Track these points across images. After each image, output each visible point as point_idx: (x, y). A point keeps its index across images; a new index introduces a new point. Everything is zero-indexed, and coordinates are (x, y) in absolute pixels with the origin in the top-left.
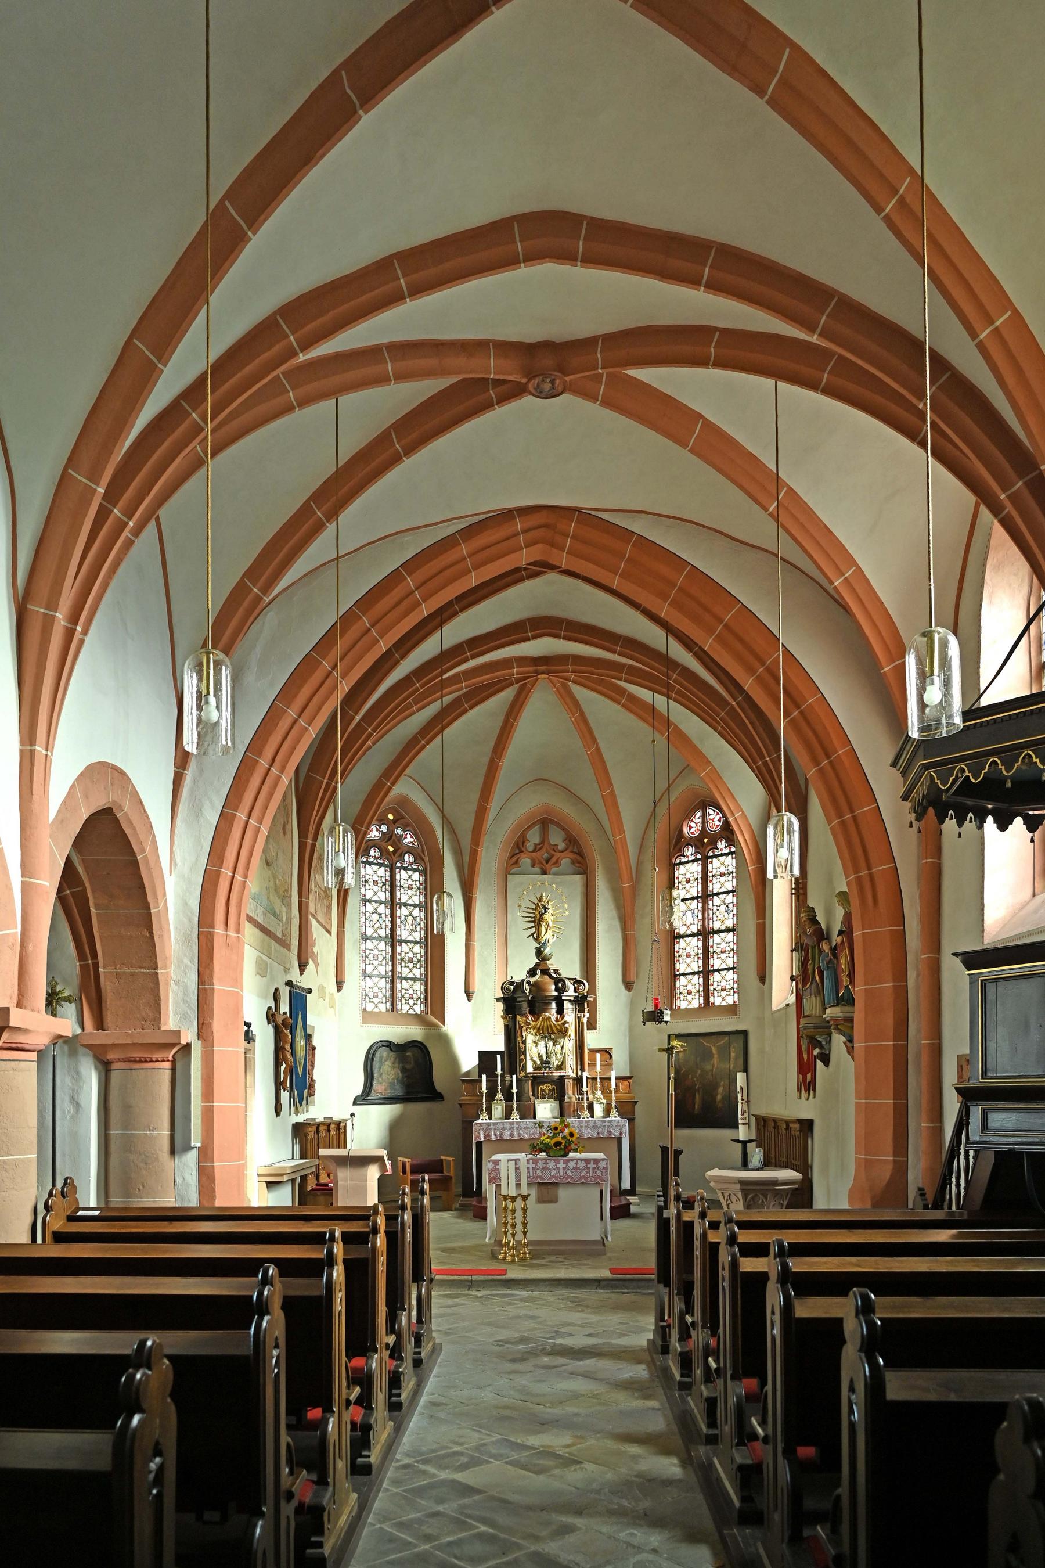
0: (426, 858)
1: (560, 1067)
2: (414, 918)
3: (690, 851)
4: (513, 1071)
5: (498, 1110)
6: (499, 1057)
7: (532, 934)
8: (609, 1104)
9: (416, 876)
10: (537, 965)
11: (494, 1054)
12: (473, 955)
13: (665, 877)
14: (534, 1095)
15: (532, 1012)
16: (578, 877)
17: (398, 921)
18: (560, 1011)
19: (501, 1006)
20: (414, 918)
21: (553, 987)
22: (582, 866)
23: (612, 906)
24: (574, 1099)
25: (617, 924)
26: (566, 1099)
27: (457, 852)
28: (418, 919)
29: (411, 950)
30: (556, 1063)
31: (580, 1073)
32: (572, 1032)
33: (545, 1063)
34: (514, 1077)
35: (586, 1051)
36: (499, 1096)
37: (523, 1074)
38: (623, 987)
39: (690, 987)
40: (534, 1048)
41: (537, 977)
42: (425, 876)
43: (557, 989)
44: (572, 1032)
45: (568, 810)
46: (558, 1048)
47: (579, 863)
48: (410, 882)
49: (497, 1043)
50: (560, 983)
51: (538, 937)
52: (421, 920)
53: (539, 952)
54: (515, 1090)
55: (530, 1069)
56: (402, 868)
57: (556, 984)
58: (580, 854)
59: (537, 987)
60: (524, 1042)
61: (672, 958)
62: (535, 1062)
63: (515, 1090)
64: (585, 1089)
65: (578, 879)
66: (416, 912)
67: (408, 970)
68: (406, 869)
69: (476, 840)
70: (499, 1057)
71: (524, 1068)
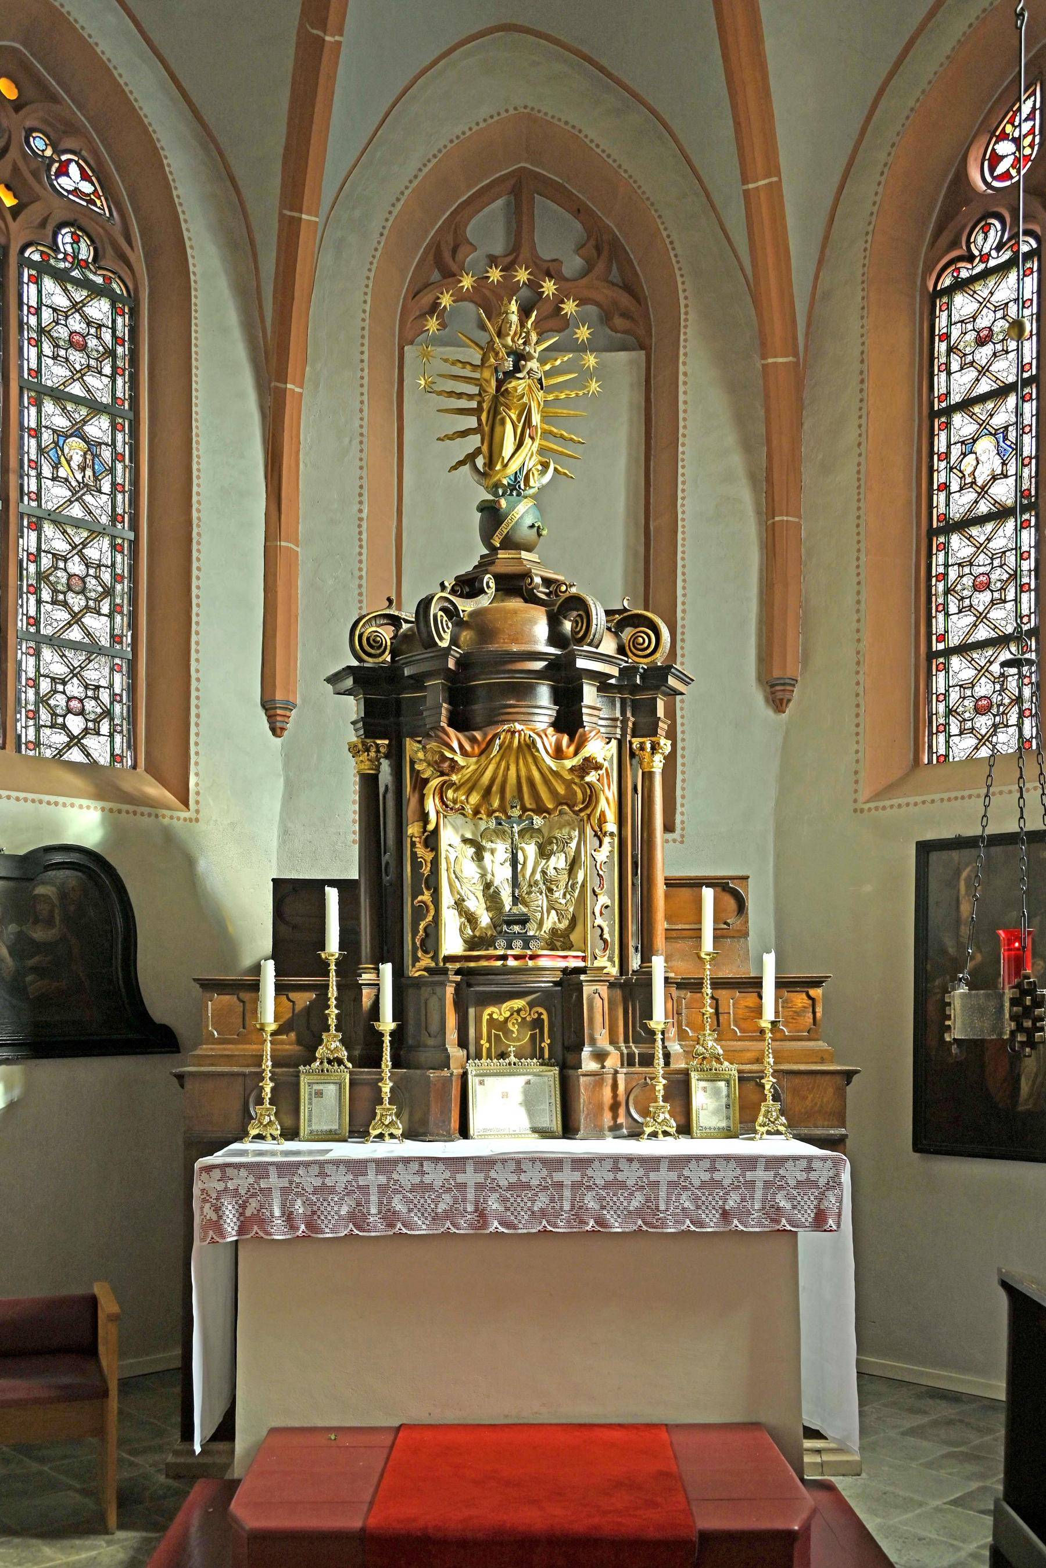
0: (137, 256)
1: (559, 940)
2: (92, 446)
3: (987, 241)
4: (388, 947)
5: (324, 1096)
6: (332, 895)
7: (471, 458)
8: (750, 1081)
9: (99, 309)
10: (485, 564)
11: (317, 886)
12: (291, 583)
13: (902, 336)
14: (463, 1043)
15: (460, 722)
16: (623, 356)
17: (31, 445)
18: (569, 721)
19: (352, 707)
20: (92, 446)
21: (541, 630)
22: (634, 317)
23: (731, 439)
24: (613, 1061)
25: (745, 496)
26: (589, 1064)
27: (240, 246)
28: (106, 454)
29: (78, 550)
30: (551, 921)
31: (635, 962)
32: (607, 805)
33: (510, 924)
34: (387, 969)
35: (660, 889)
36: (332, 1044)
37: (426, 961)
38: (758, 698)
39: (984, 688)
40: (469, 873)
41: (483, 601)
42: (134, 313)
43: (556, 638)
44: (607, 805)
45: (600, 131)
46: (558, 862)
47: (626, 315)
48: (76, 323)
49: (337, 854)
50: (565, 607)
51: (490, 463)
52: (117, 457)
53: (492, 516)
54: (387, 1024)
55: (452, 943)
56: (43, 269)
57: (554, 622)
58: (631, 288)
59: (482, 627)
60: (432, 840)
61: (923, 598)
62: (471, 919)
63: (387, 1024)
64: (658, 1019)
65: (624, 362)
66: (98, 428)
67: (63, 615)
68: (61, 277)
69: (294, 192)
70: (332, 895)
71: (431, 940)
